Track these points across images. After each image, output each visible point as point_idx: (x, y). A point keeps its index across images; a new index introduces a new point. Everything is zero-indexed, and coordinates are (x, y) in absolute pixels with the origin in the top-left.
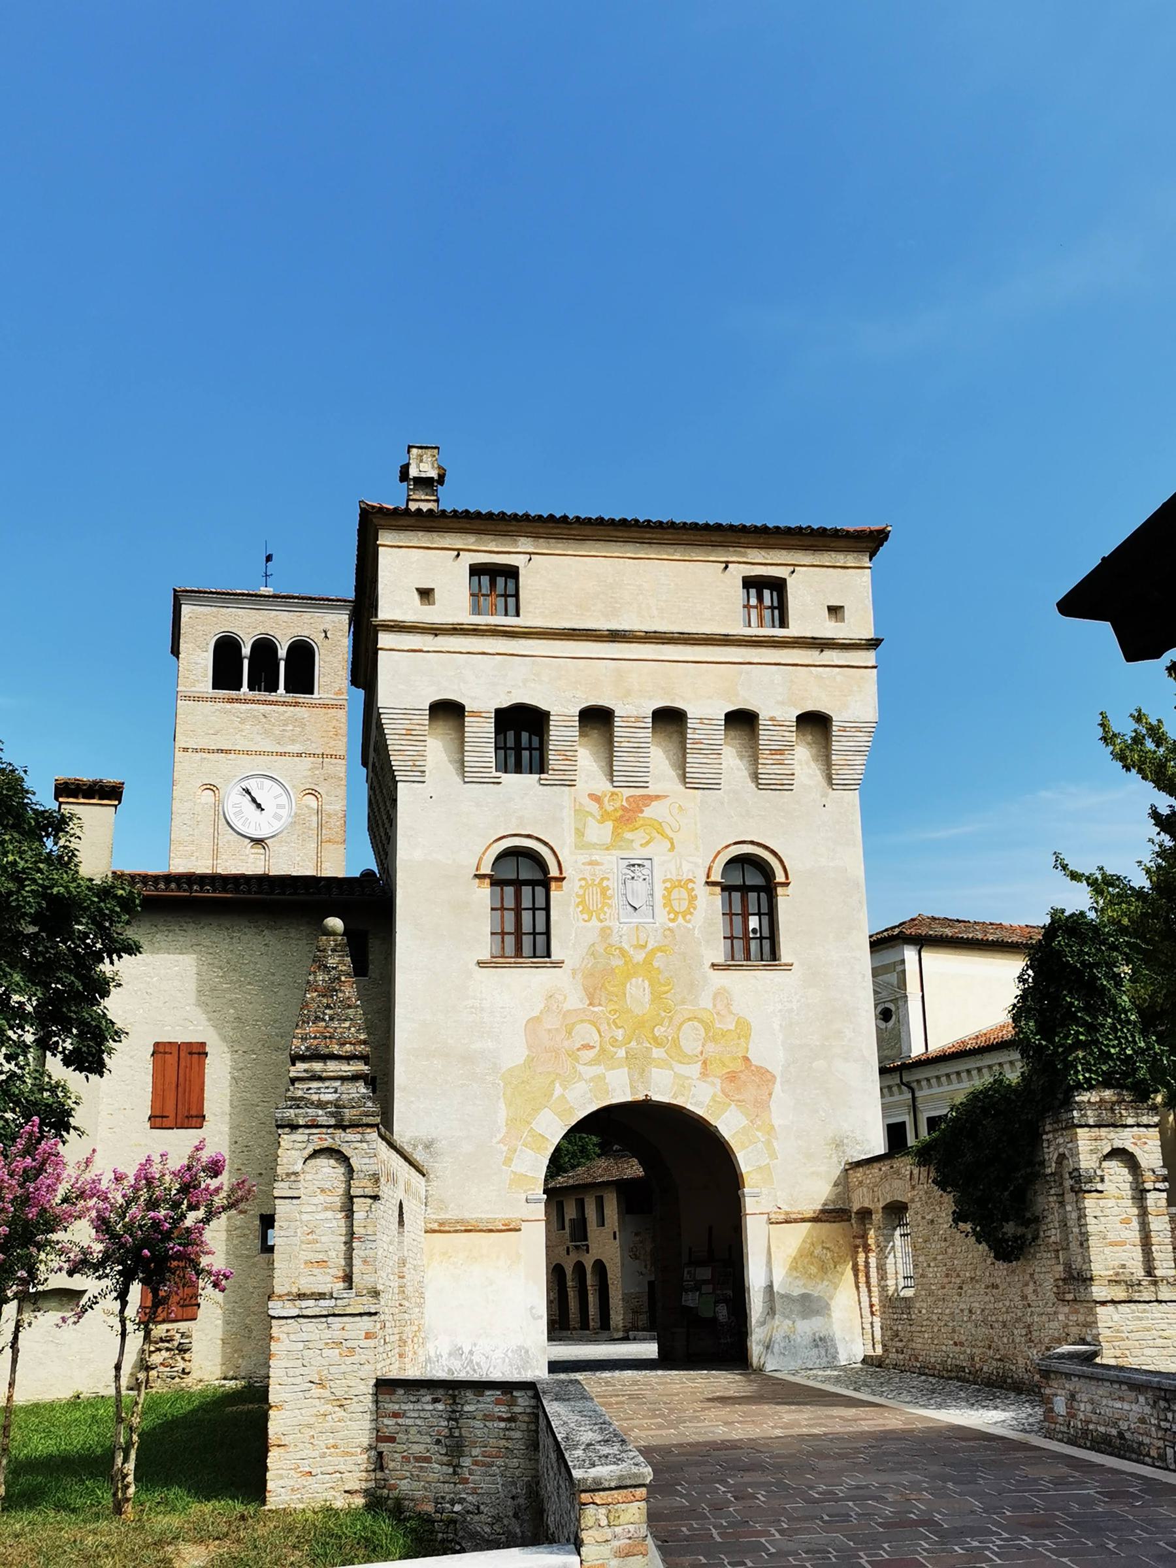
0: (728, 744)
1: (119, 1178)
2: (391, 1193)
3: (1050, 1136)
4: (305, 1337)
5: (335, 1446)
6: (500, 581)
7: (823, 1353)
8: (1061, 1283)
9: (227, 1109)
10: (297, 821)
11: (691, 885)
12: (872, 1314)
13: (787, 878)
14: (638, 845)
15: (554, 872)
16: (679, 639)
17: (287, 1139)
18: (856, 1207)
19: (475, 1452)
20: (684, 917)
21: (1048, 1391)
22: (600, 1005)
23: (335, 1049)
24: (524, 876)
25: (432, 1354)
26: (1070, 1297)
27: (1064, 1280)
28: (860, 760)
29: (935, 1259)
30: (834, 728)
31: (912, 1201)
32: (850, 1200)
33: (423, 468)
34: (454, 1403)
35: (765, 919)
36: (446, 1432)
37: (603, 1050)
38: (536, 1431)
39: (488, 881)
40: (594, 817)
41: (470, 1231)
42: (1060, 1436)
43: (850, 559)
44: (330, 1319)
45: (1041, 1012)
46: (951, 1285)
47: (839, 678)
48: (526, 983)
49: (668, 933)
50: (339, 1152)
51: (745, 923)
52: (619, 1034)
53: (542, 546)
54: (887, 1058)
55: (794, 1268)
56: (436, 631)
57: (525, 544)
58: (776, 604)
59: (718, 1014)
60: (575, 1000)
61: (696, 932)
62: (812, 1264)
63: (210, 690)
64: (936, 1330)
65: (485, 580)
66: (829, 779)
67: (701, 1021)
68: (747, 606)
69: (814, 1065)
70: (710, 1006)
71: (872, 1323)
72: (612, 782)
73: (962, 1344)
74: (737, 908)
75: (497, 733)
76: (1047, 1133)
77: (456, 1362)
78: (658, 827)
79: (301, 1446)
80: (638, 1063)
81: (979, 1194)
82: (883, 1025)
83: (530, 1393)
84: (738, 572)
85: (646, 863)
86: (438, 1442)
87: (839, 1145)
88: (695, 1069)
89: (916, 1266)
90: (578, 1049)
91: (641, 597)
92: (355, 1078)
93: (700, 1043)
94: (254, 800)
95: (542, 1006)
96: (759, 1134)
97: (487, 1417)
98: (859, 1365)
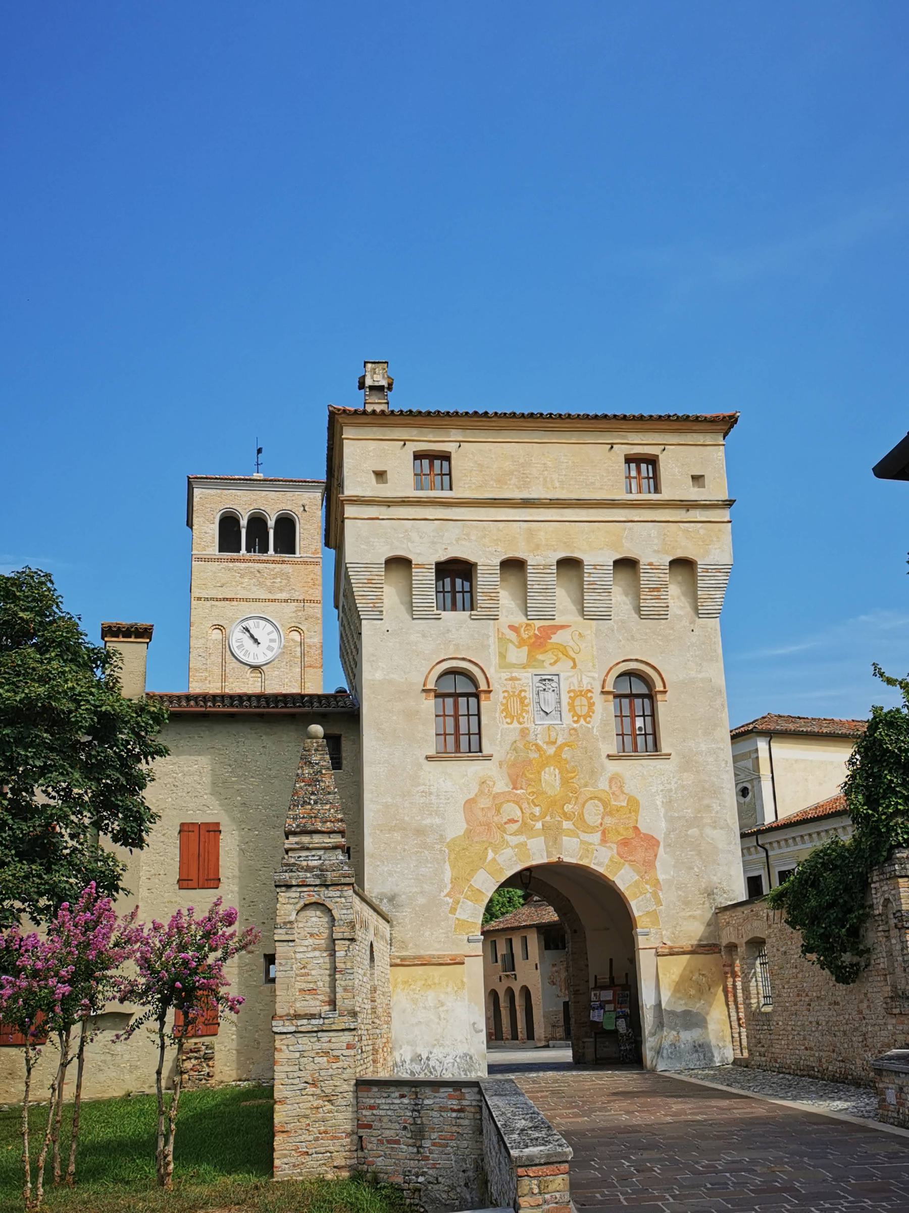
1: (156, 927)
2: (364, 936)
3: (877, 885)
4: (301, 1048)
5: (326, 1132)
6: (437, 463)
8: (889, 1000)
9: (237, 873)
10: (285, 651)
11: (589, 695)
12: (740, 1025)
13: (665, 687)
14: (548, 664)
15: (483, 686)
17: (283, 896)
18: (724, 942)
19: (434, 1136)
20: (585, 719)
21: (881, 1085)
22: (522, 788)
23: (319, 826)
25: (398, 1060)
26: (897, 1011)
27: (892, 998)
29: (788, 982)
30: (699, 570)
33: (377, 378)
34: (417, 1098)
35: (648, 719)
36: (411, 1121)
37: (525, 824)
38: (481, 1119)
39: (432, 694)
41: (425, 965)
42: (892, 1120)
43: (708, 439)
44: (320, 1034)
45: (867, 787)
47: (702, 532)
49: (572, 732)
50: (323, 905)
51: (633, 723)
52: (537, 811)
53: (470, 435)
54: (746, 826)
56: (388, 503)
57: (456, 435)
58: (651, 475)
59: (613, 794)
60: (501, 785)
61: (595, 730)
63: (217, 553)
65: (426, 462)
66: (696, 610)
67: (600, 800)
68: (629, 477)
70: (607, 788)
71: (740, 1033)
72: (527, 615)
73: (811, 1049)
74: (626, 712)
75: (437, 580)
76: (875, 883)
77: (416, 1066)
78: (563, 650)
79: (300, 1132)
80: (553, 834)
81: (822, 931)
82: (742, 800)
83: (476, 1090)
84: (621, 451)
86: (405, 1128)
87: (710, 893)
88: (596, 838)
90: (506, 823)
92: (335, 848)
94: (252, 636)
95: (476, 791)
96: (648, 887)
97: (442, 1109)
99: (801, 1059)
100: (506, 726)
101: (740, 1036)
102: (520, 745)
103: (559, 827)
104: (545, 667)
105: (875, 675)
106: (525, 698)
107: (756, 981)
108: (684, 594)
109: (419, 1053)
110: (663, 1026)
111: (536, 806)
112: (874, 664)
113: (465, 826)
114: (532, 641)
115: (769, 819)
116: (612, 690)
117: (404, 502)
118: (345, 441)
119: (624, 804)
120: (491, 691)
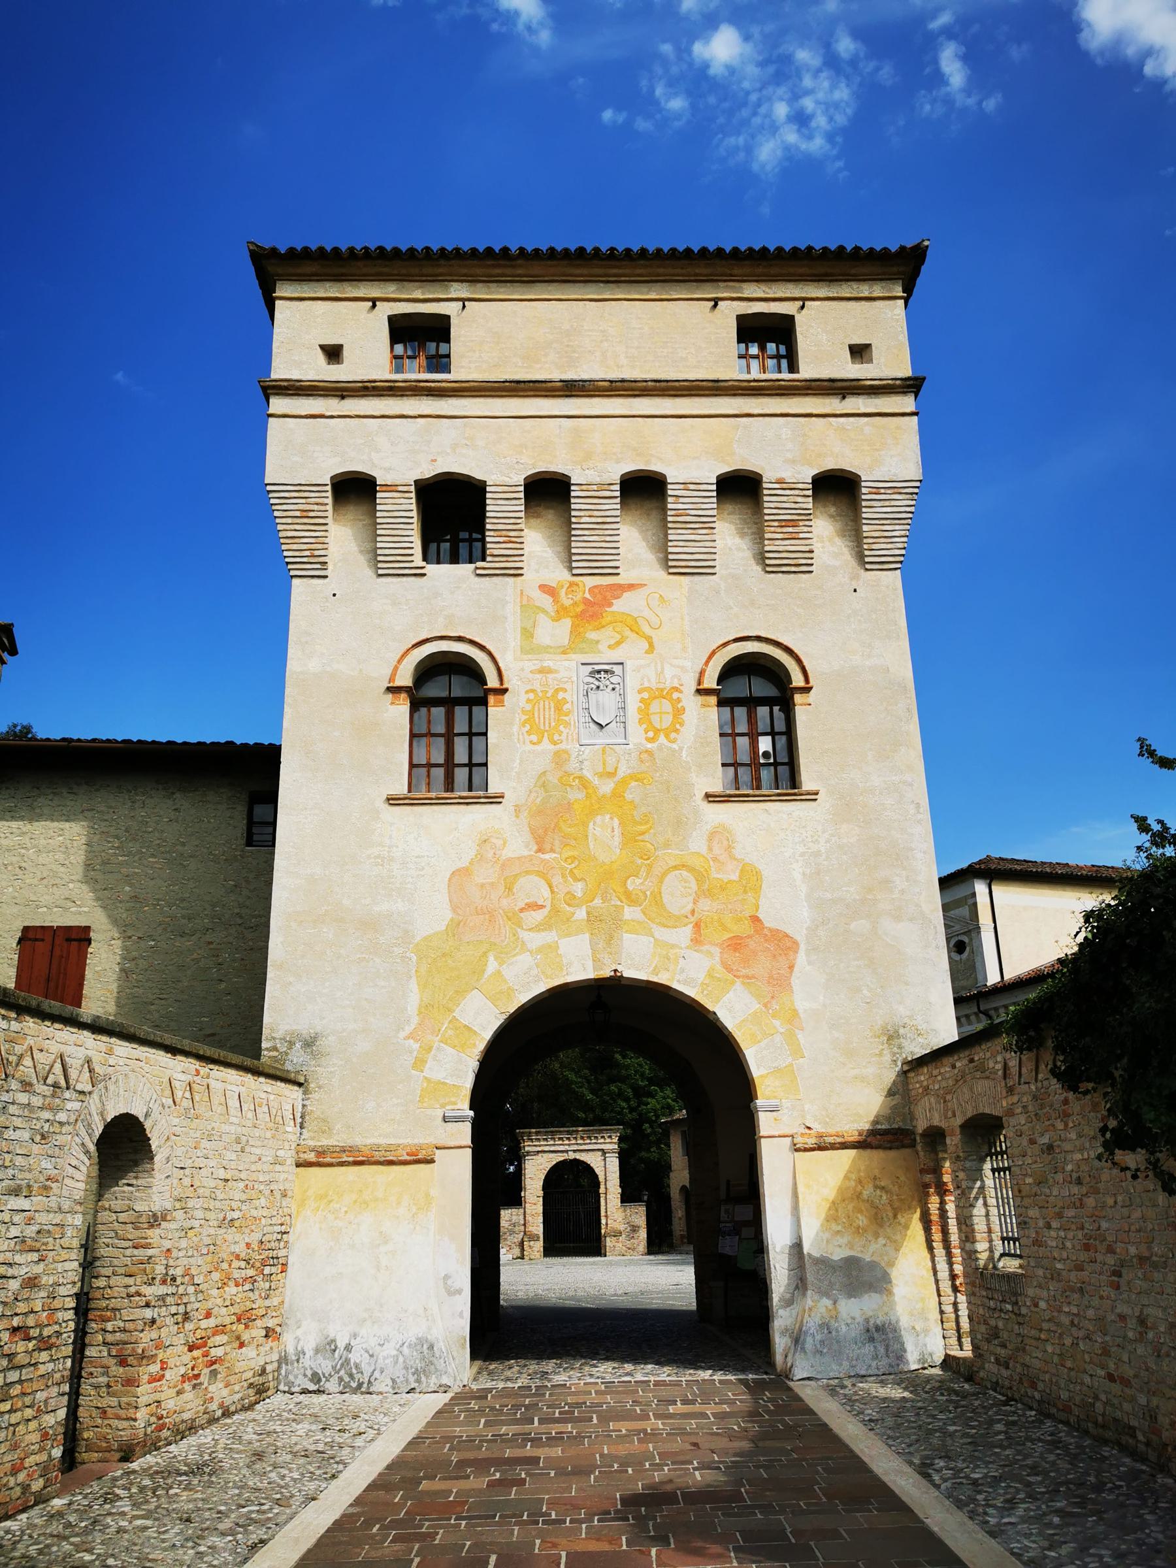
0: (723, 519)
7: (882, 1350)
11: (675, 695)
12: (955, 1289)
13: (807, 680)
14: (604, 646)
15: (492, 682)
16: (654, 389)
18: (921, 1126)
20: (667, 736)
22: (552, 851)
24: (457, 692)
25: (291, 1350)
28: (900, 530)
29: (1060, 1215)
30: (864, 490)
31: (1010, 1113)
32: (912, 1117)
35: (782, 741)
37: (555, 911)
40: (544, 611)
43: (877, 290)
46: (1097, 1267)
47: (867, 430)
48: (452, 827)
51: (754, 745)
52: (578, 889)
53: (481, 291)
54: (964, 988)
55: (832, 1217)
56: (342, 391)
57: (459, 290)
59: (715, 859)
60: (518, 845)
61: (684, 754)
62: (860, 1211)
64: (1068, 1341)
66: (861, 558)
67: (691, 869)
69: (852, 926)
70: (704, 850)
71: (955, 1304)
72: (571, 568)
74: (742, 727)
78: (633, 625)
80: (606, 927)
82: (957, 957)
84: (730, 312)
85: (616, 668)
87: (892, 1037)
88: (684, 934)
89: (1022, 1225)
90: (522, 910)
91: (606, 344)
93: (691, 898)
95: (472, 854)
96: (777, 1023)
98: (937, 1371)
99: (1096, 1398)
100: (529, 747)
101: (956, 1310)
102: (553, 779)
103: (617, 922)
104: (599, 652)
105: (1141, 755)
106: (565, 701)
107: (985, 1204)
108: (842, 534)
109: (332, 1336)
110: (805, 1289)
111: (577, 880)
112: (1139, 739)
113: (449, 915)
114: (579, 610)
115: (993, 978)
116: (714, 685)
117: (368, 389)
118: (277, 302)
119: (734, 877)
120: (506, 690)
